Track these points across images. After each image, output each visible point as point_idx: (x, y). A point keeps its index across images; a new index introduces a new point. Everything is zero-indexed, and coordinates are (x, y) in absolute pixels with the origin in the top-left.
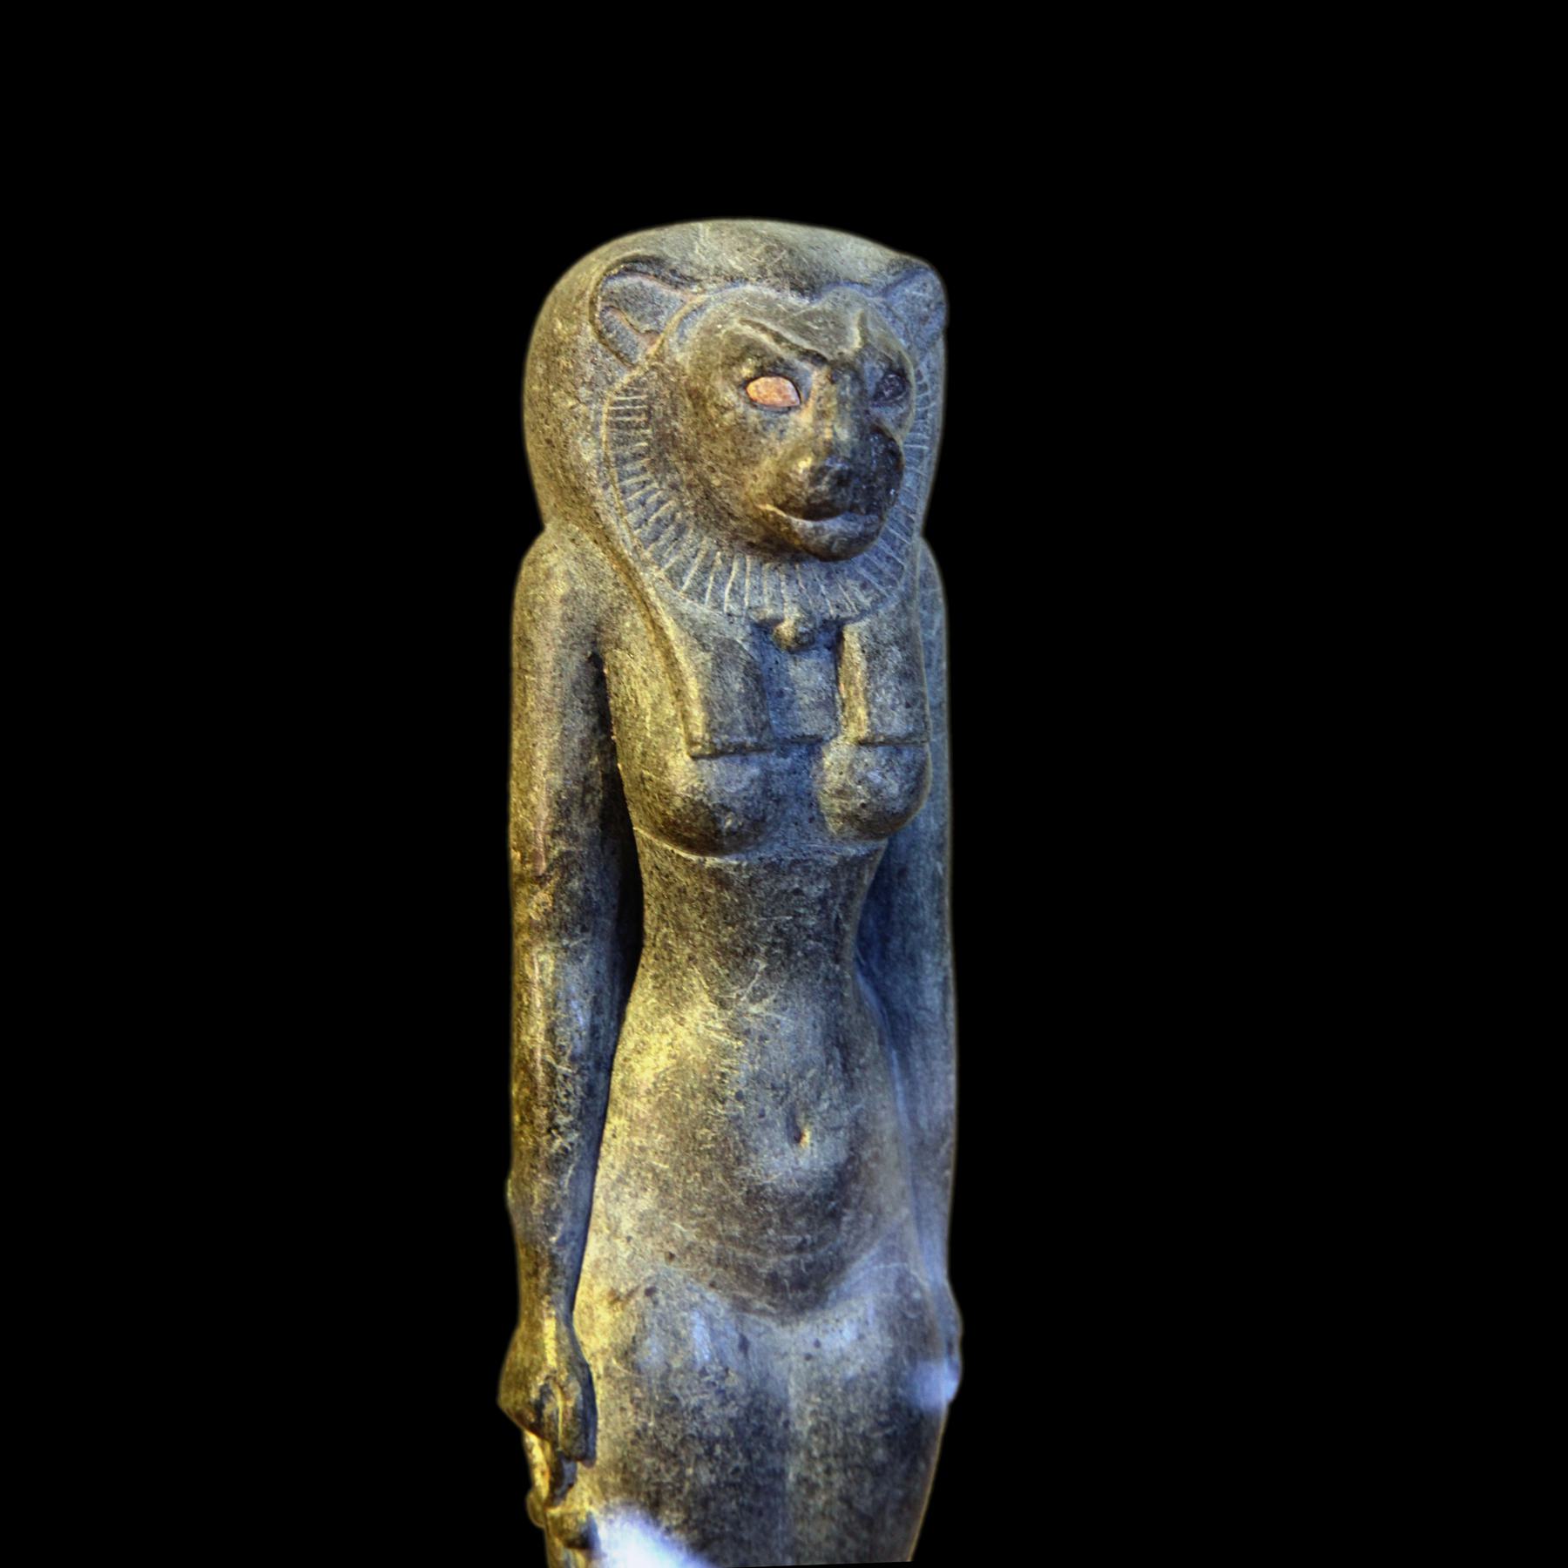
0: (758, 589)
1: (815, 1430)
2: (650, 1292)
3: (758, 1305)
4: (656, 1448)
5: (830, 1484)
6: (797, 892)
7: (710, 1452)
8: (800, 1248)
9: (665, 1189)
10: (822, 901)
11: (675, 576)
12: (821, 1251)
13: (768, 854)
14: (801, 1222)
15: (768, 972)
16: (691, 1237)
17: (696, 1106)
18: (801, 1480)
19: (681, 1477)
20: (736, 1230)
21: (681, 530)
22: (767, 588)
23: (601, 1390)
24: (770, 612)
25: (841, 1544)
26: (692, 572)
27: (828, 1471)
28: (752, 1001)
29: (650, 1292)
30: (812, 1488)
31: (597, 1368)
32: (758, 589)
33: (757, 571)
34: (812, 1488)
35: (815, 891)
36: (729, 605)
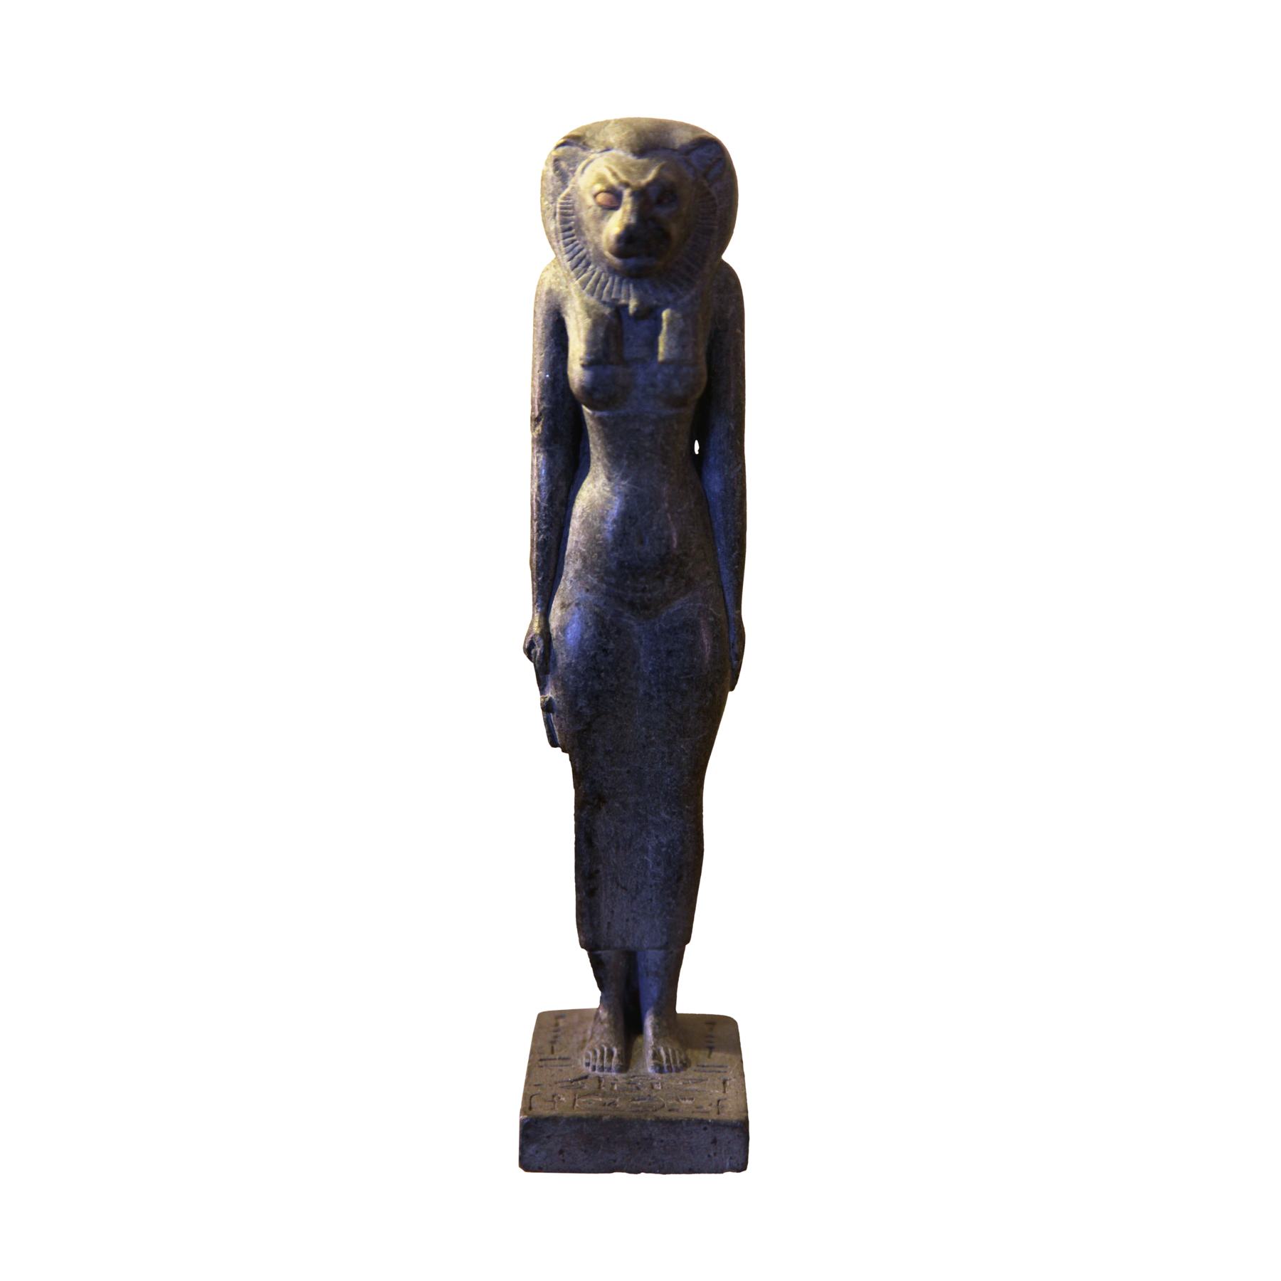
0: (619, 291)
1: (652, 672)
2: (577, 605)
3: (626, 615)
4: (575, 672)
5: (659, 697)
6: (638, 430)
7: (599, 676)
8: (644, 590)
9: (584, 560)
10: (652, 435)
11: (584, 284)
12: (655, 593)
13: (622, 412)
14: (642, 579)
15: (629, 466)
16: (595, 582)
17: (596, 524)
18: (646, 694)
19: (586, 685)
20: (613, 580)
21: (588, 264)
22: (624, 290)
23: (555, 644)
24: (623, 301)
25: (668, 724)
26: (591, 282)
27: (659, 691)
28: (622, 479)
29: (577, 605)
30: (652, 698)
31: (554, 634)
32: (619, 291)
33: (620, 283)
34: (652, 698)
35: (648, 429)
36: (604, 298)
